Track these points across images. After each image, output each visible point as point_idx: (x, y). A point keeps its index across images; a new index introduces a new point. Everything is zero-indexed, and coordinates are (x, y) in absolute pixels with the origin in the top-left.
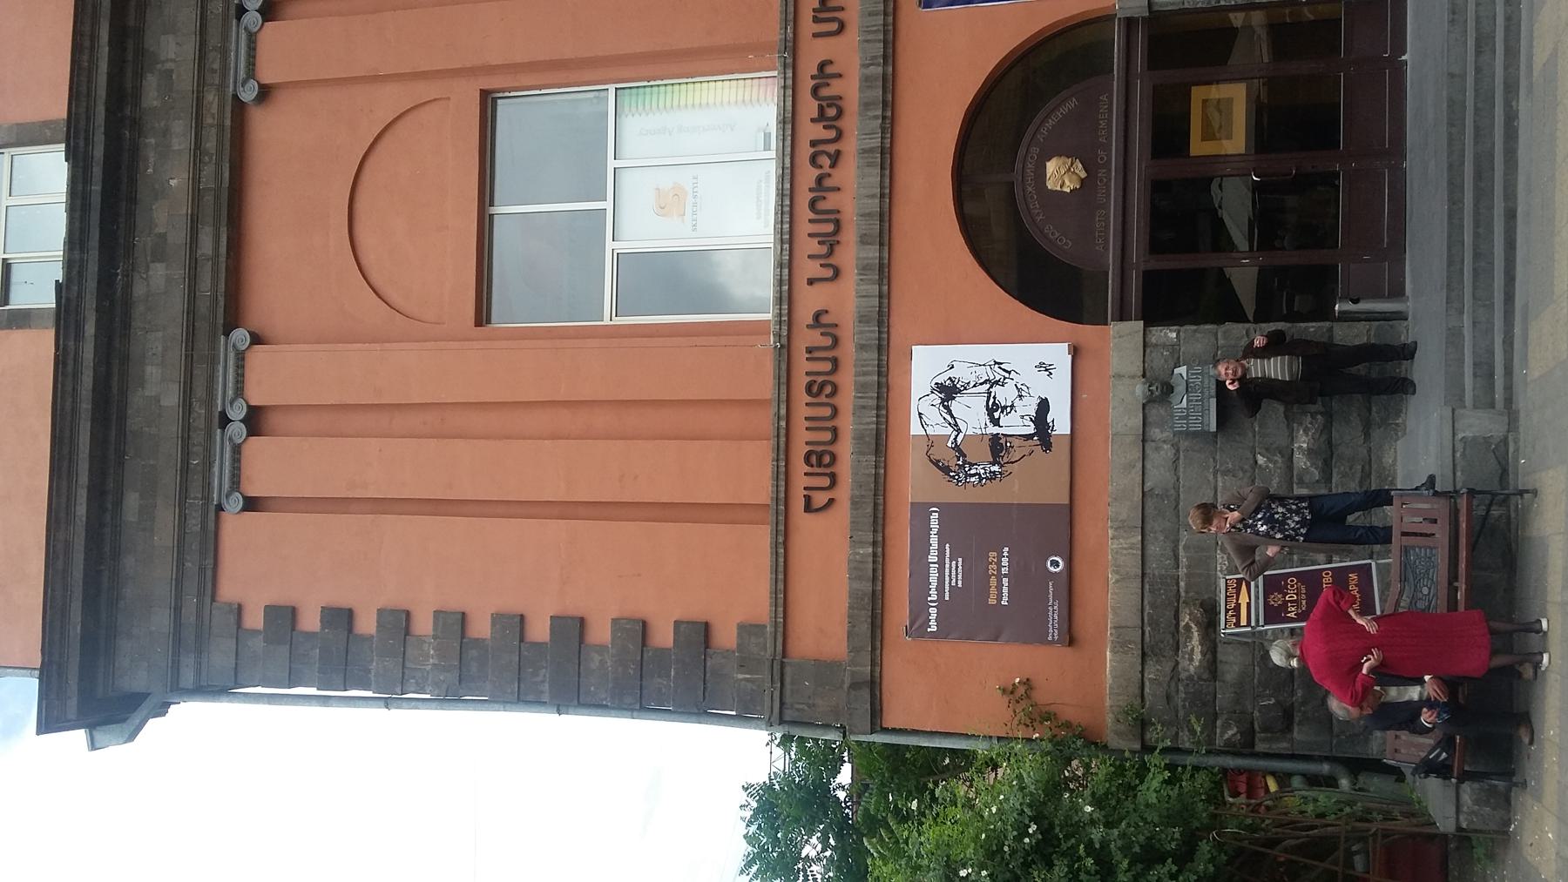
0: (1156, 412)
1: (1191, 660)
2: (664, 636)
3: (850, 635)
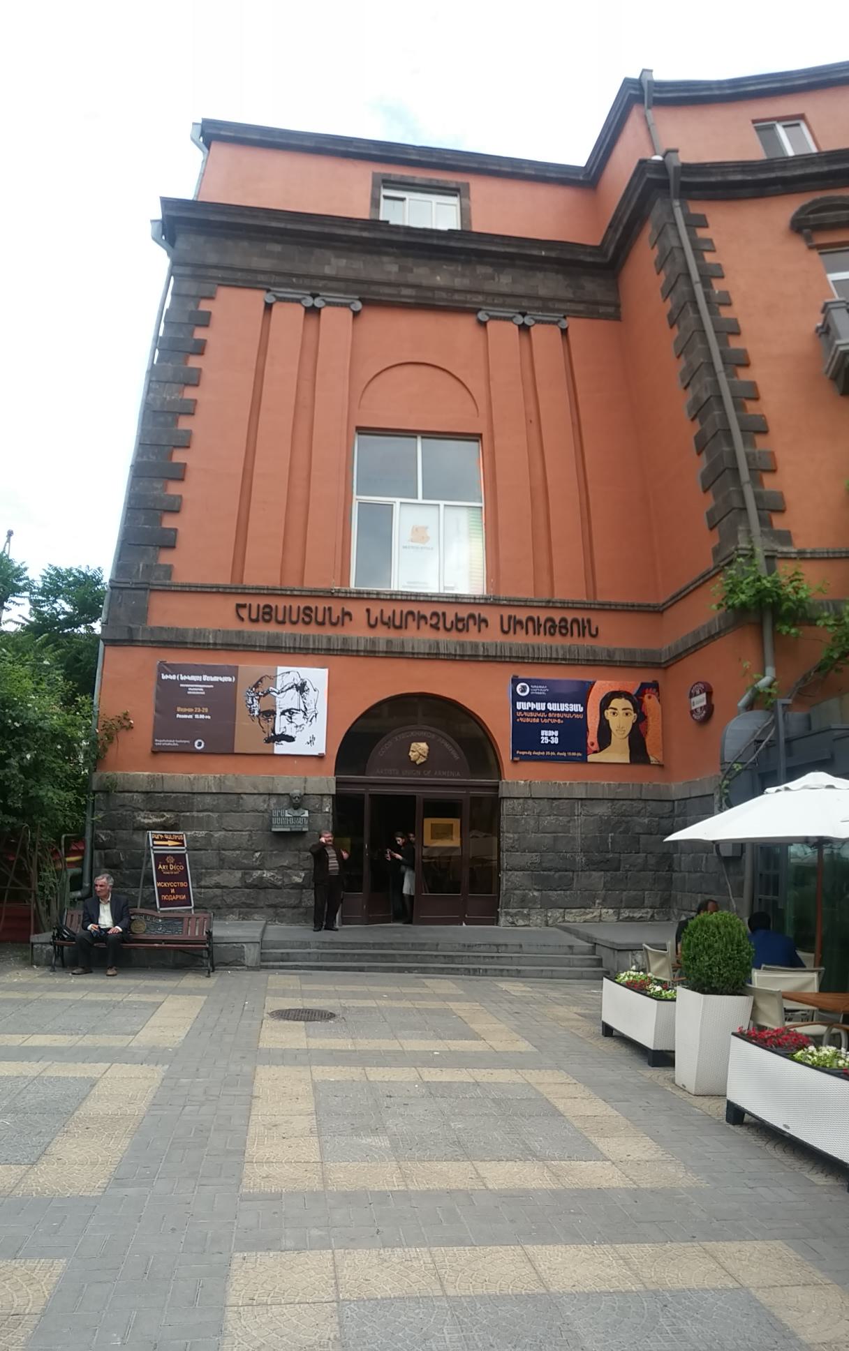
0: (285, 800)
1: (145, 818)
3: (162, 628)
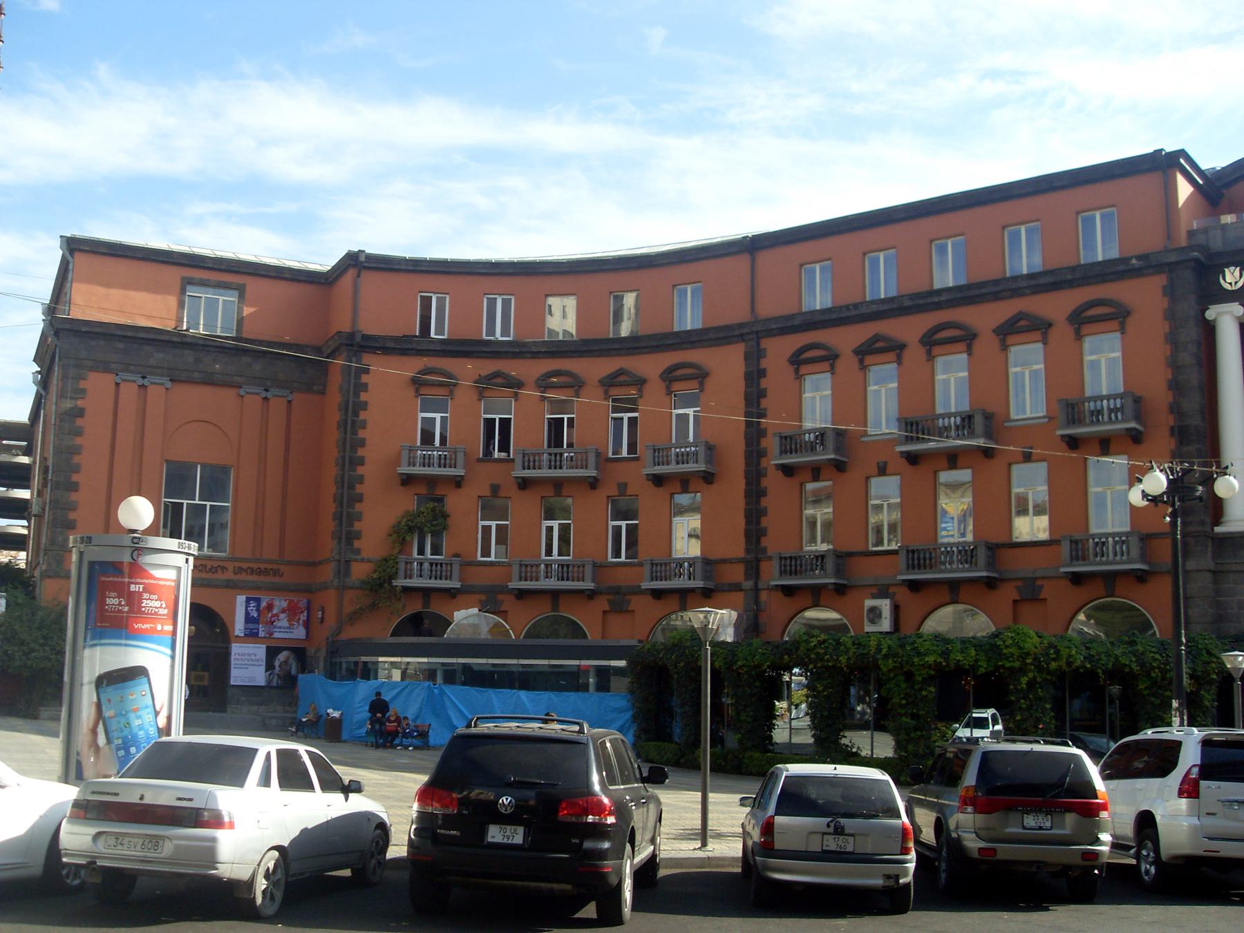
2: (72, 516)
